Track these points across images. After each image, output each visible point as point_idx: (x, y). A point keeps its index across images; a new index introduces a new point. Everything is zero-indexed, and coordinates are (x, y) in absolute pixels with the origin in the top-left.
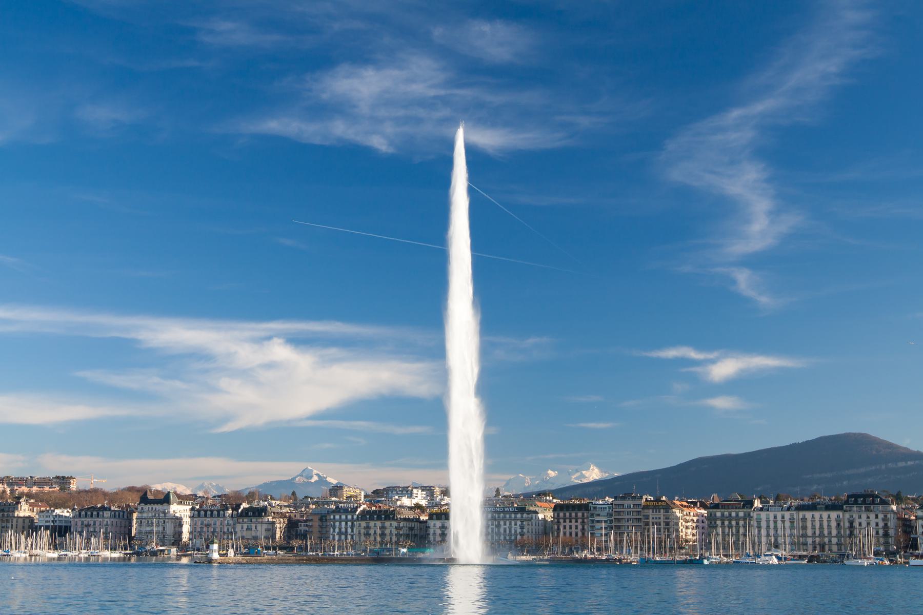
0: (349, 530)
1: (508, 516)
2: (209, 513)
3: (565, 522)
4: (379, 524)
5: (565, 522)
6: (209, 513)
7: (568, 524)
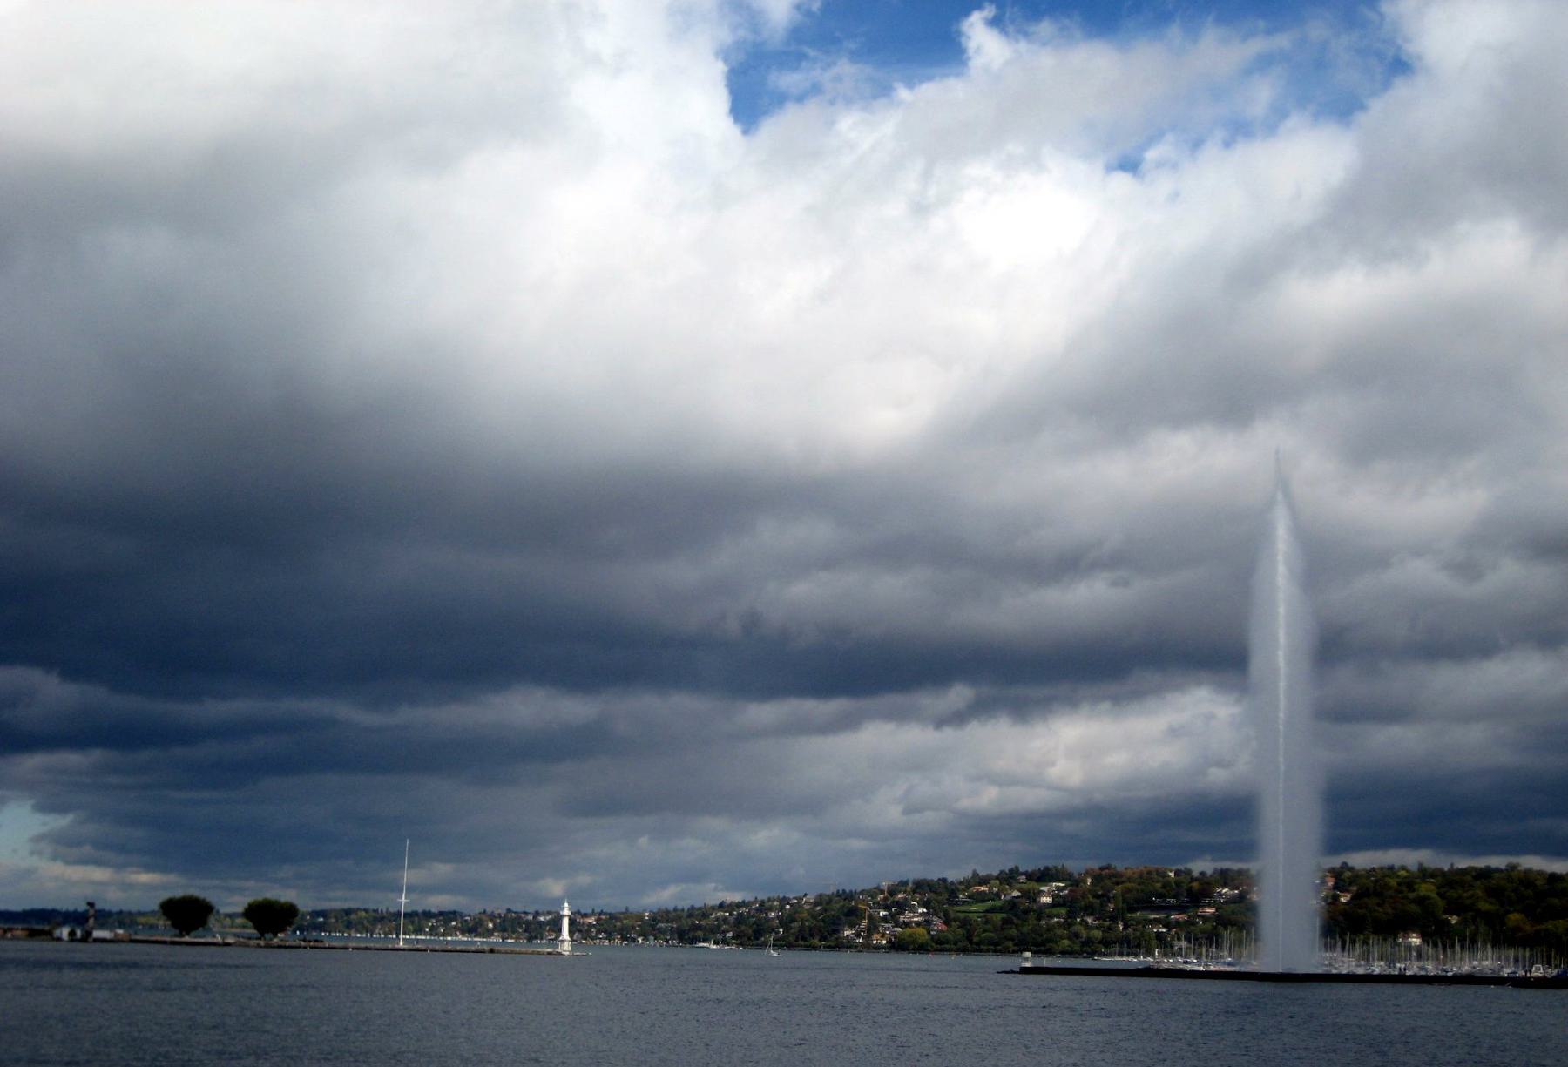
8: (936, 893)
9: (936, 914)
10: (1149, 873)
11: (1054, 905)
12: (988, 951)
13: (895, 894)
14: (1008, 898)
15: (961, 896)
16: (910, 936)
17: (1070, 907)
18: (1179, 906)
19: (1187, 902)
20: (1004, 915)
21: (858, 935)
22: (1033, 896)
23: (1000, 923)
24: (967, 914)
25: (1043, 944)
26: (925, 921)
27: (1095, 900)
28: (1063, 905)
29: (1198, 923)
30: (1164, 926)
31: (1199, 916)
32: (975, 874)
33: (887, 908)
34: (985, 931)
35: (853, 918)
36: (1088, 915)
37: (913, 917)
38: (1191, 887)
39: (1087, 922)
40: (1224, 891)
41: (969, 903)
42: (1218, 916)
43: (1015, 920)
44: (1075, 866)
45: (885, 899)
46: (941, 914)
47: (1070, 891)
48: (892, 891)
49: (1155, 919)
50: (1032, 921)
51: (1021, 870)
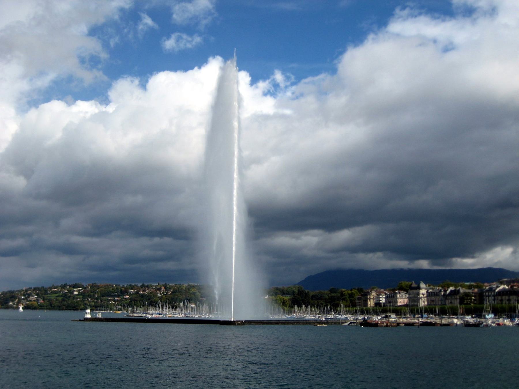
2: (433, 294)
4: (507, 297)
6: (433, 294)
8: (40, 291)
9: (40, 297)
10: (107, 285)
11: (78, 295)
12: (57, 309)
13: (28, 291)
14: (64, 293)
15: (49, 292)
16: (31, 304)
17: (84, 295)
18: (118, 295)
19: (120, 294)
20: (63, 298)
21: (14, 304)
22: (72, 292)
23: (61, 300)
24: (51, 298)
25: (75, 307)
26: (37, 300)
27: (91, 293)
28: (81, 295)
29: (124, 300)
30: (113, 301)
31: (124, 298)
32: (53, 285)
33: (24, 295)
34: (56, 303)
35: (13, 299)
36: (89, 298)
37: (33, 298)
38: (122, 289)
39: (89, 300)
40: (132, 291)
41: (51, 294)
42: (131, 298)
43: (66, 299)
44: (85, 284)
45: (24, 293)
46: (42, 298)
47: (84, 290)
48: (26, 291)
49: (110, 299)
50: (71, 299)
51: (68, 284)
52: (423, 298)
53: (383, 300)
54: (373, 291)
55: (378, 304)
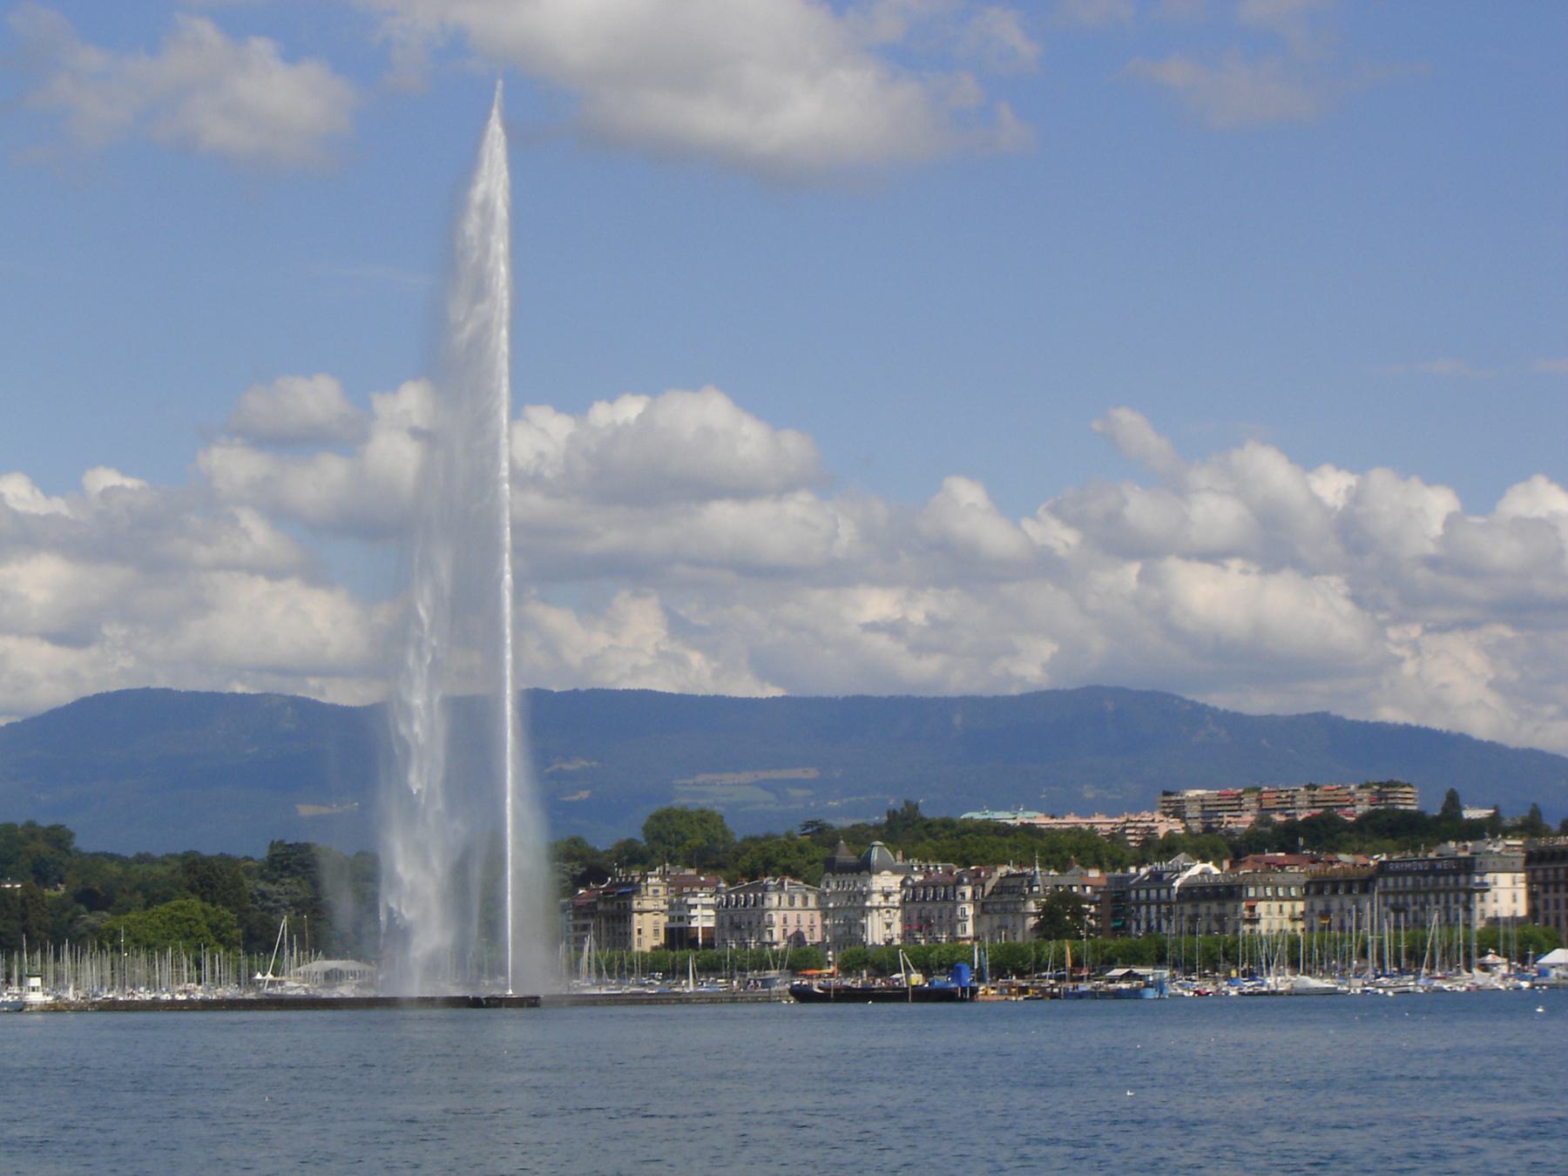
0: (1164, 923)
1: (1442, 880)
3: (1546, 891)
5: (1546, 891)
7: (1551, 896)
52: (885, 907)
53: (702, 919)
54: (651, 877)
55: (678, 936)
